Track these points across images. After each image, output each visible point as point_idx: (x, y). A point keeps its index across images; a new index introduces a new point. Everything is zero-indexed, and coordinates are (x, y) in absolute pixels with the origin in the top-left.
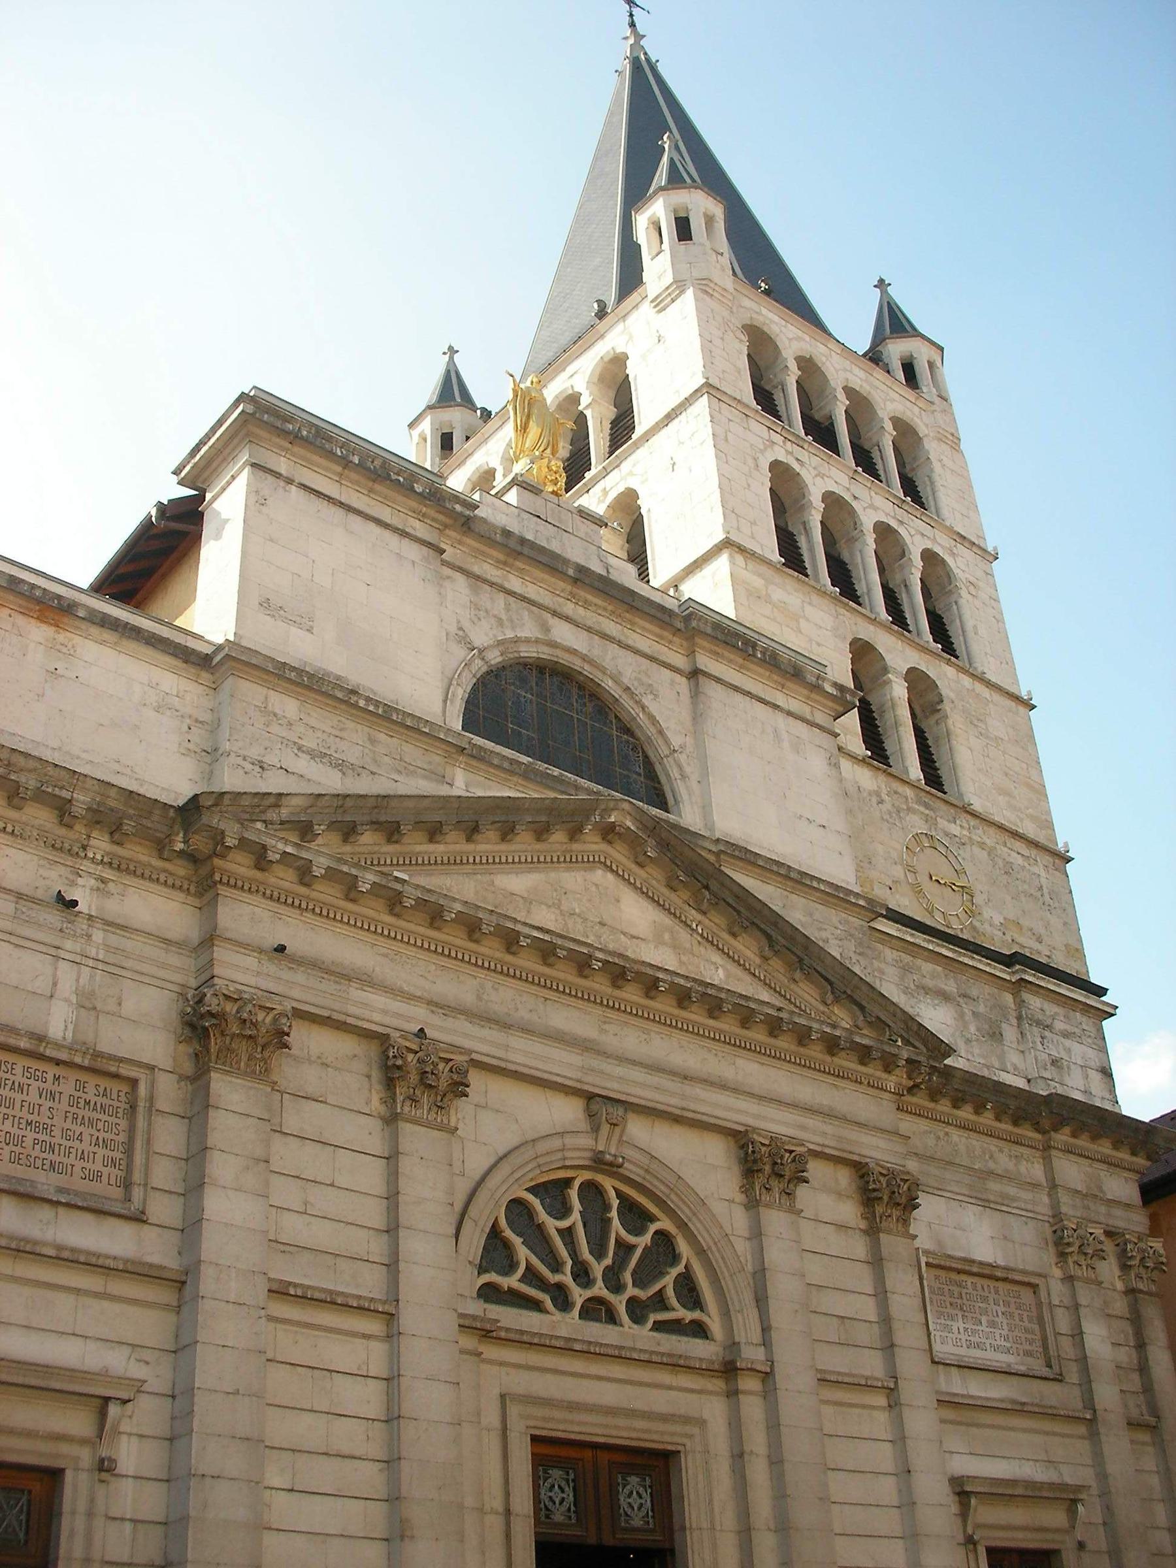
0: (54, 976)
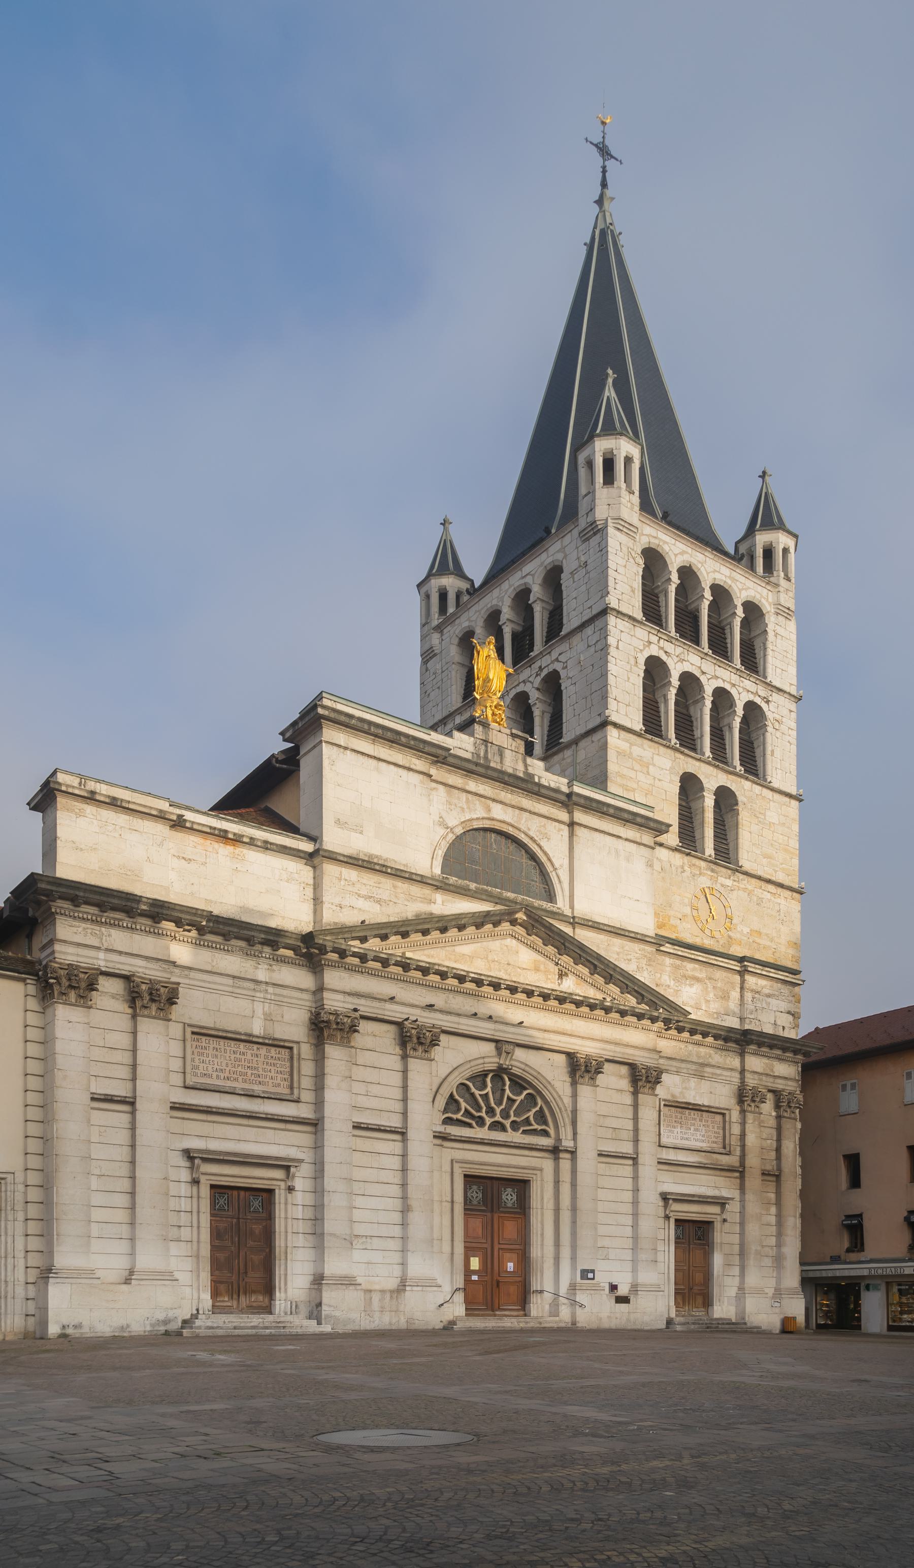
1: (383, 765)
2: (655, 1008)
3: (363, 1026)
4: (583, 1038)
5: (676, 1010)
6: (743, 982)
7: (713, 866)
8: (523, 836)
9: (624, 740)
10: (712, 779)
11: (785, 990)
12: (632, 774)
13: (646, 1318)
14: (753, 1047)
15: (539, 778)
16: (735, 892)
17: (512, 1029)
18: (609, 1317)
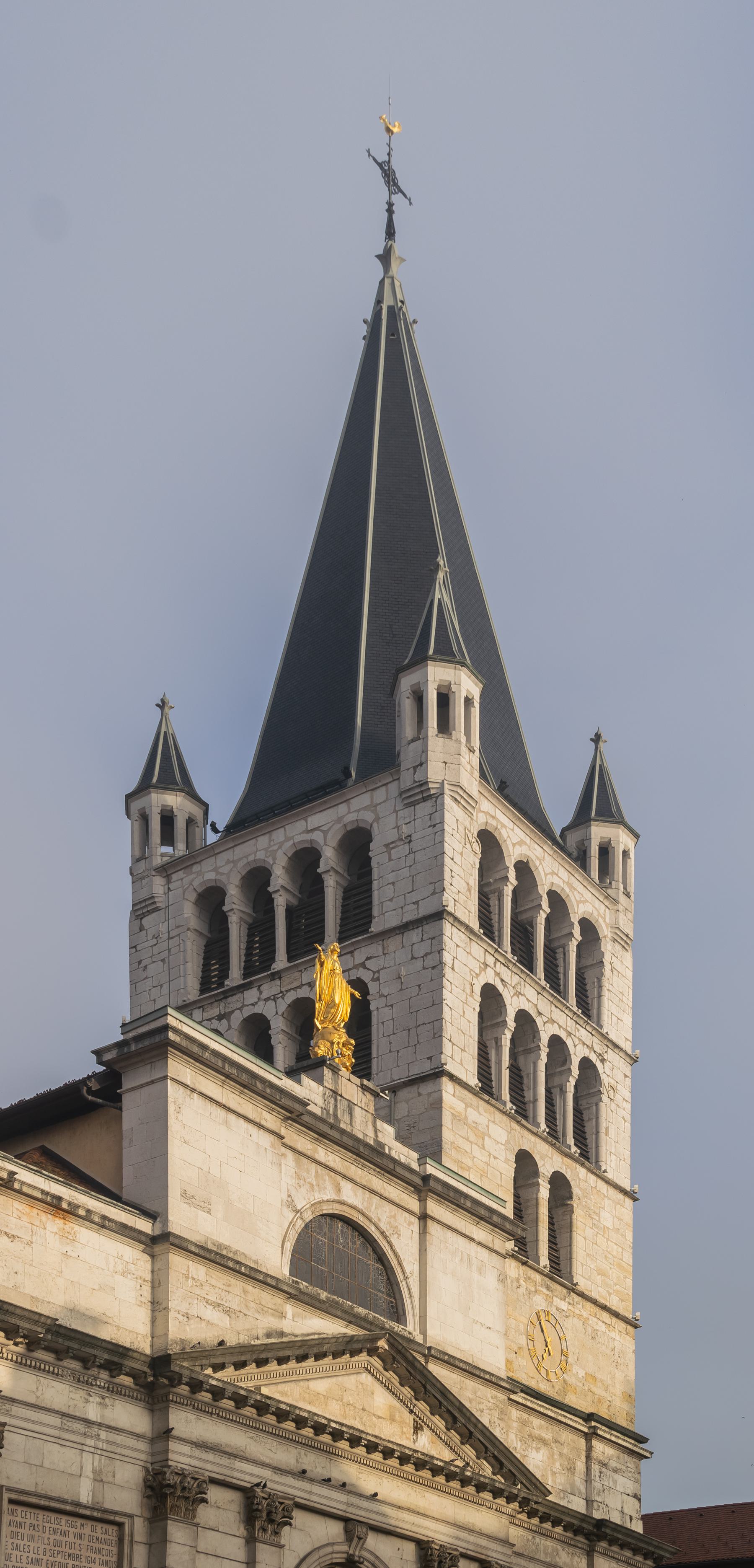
0: (81, 1462)
1: (232, 1117)
2: (508, 1480)
3: (214, 1494)
6: (589, 1449)
7: (549, 1282)
10: (549, 1161)
11: (631, 1462)
14: (604, 1544)
15: (390, 1149)
16: (570, 1319)
17: (366, 1504)
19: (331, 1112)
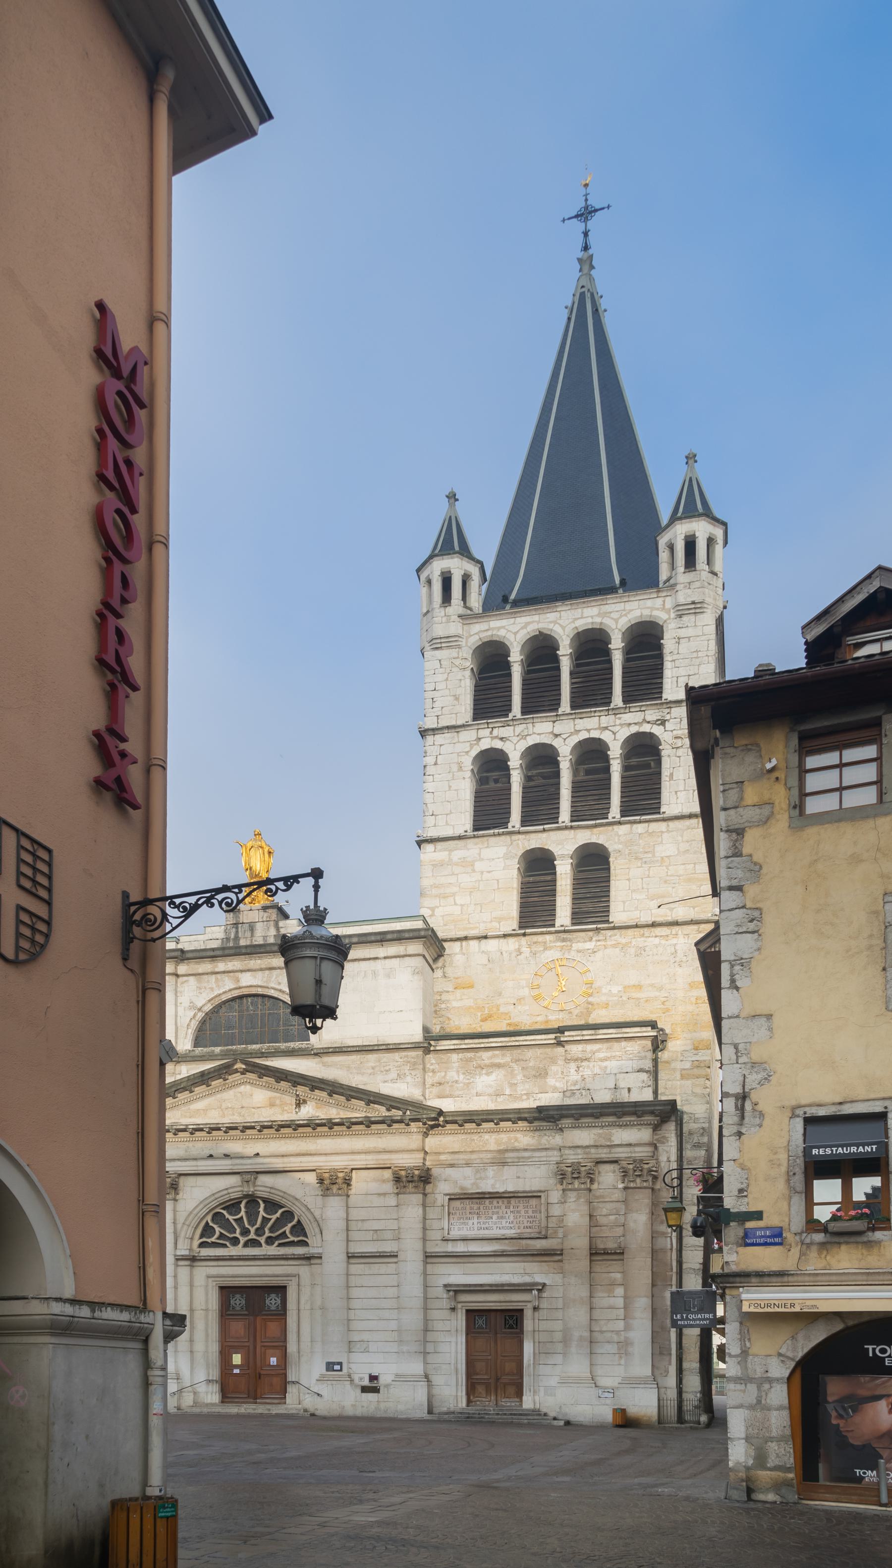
4: (326, 1154)
5: (423, 1109)
8: (272, 991)
9: (440, 851)
12: (452, 879)
13: (401, 1407)
17: (249, 1161)
18: (352, 1405)
19: (232, 936)
